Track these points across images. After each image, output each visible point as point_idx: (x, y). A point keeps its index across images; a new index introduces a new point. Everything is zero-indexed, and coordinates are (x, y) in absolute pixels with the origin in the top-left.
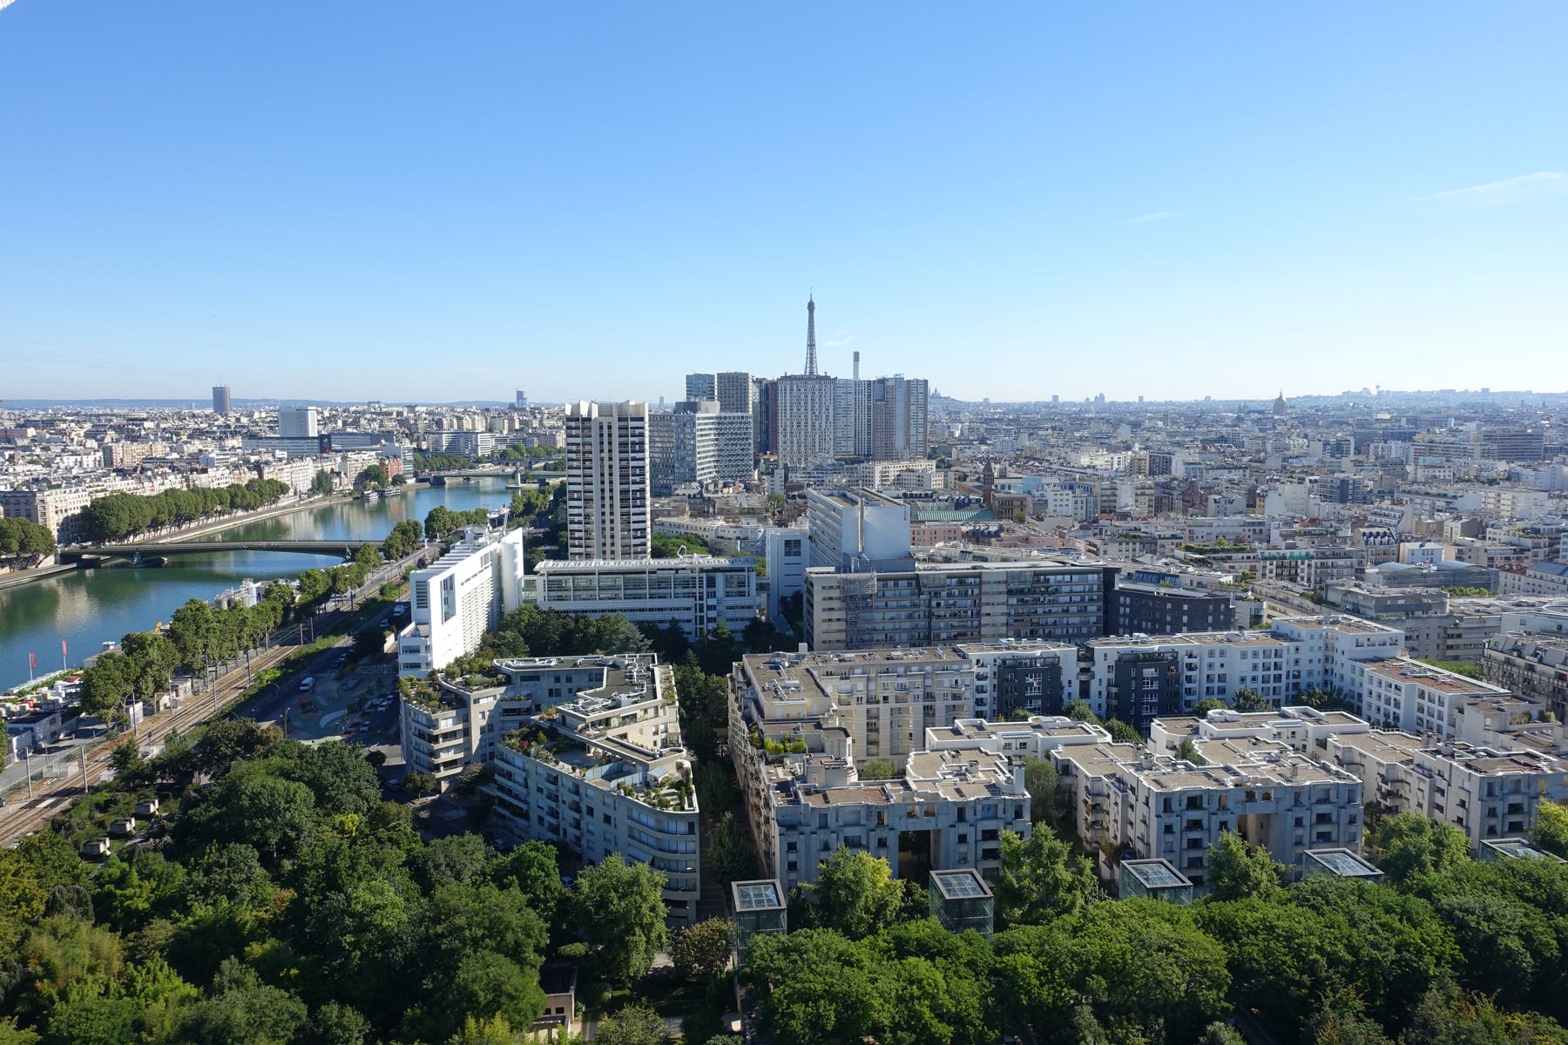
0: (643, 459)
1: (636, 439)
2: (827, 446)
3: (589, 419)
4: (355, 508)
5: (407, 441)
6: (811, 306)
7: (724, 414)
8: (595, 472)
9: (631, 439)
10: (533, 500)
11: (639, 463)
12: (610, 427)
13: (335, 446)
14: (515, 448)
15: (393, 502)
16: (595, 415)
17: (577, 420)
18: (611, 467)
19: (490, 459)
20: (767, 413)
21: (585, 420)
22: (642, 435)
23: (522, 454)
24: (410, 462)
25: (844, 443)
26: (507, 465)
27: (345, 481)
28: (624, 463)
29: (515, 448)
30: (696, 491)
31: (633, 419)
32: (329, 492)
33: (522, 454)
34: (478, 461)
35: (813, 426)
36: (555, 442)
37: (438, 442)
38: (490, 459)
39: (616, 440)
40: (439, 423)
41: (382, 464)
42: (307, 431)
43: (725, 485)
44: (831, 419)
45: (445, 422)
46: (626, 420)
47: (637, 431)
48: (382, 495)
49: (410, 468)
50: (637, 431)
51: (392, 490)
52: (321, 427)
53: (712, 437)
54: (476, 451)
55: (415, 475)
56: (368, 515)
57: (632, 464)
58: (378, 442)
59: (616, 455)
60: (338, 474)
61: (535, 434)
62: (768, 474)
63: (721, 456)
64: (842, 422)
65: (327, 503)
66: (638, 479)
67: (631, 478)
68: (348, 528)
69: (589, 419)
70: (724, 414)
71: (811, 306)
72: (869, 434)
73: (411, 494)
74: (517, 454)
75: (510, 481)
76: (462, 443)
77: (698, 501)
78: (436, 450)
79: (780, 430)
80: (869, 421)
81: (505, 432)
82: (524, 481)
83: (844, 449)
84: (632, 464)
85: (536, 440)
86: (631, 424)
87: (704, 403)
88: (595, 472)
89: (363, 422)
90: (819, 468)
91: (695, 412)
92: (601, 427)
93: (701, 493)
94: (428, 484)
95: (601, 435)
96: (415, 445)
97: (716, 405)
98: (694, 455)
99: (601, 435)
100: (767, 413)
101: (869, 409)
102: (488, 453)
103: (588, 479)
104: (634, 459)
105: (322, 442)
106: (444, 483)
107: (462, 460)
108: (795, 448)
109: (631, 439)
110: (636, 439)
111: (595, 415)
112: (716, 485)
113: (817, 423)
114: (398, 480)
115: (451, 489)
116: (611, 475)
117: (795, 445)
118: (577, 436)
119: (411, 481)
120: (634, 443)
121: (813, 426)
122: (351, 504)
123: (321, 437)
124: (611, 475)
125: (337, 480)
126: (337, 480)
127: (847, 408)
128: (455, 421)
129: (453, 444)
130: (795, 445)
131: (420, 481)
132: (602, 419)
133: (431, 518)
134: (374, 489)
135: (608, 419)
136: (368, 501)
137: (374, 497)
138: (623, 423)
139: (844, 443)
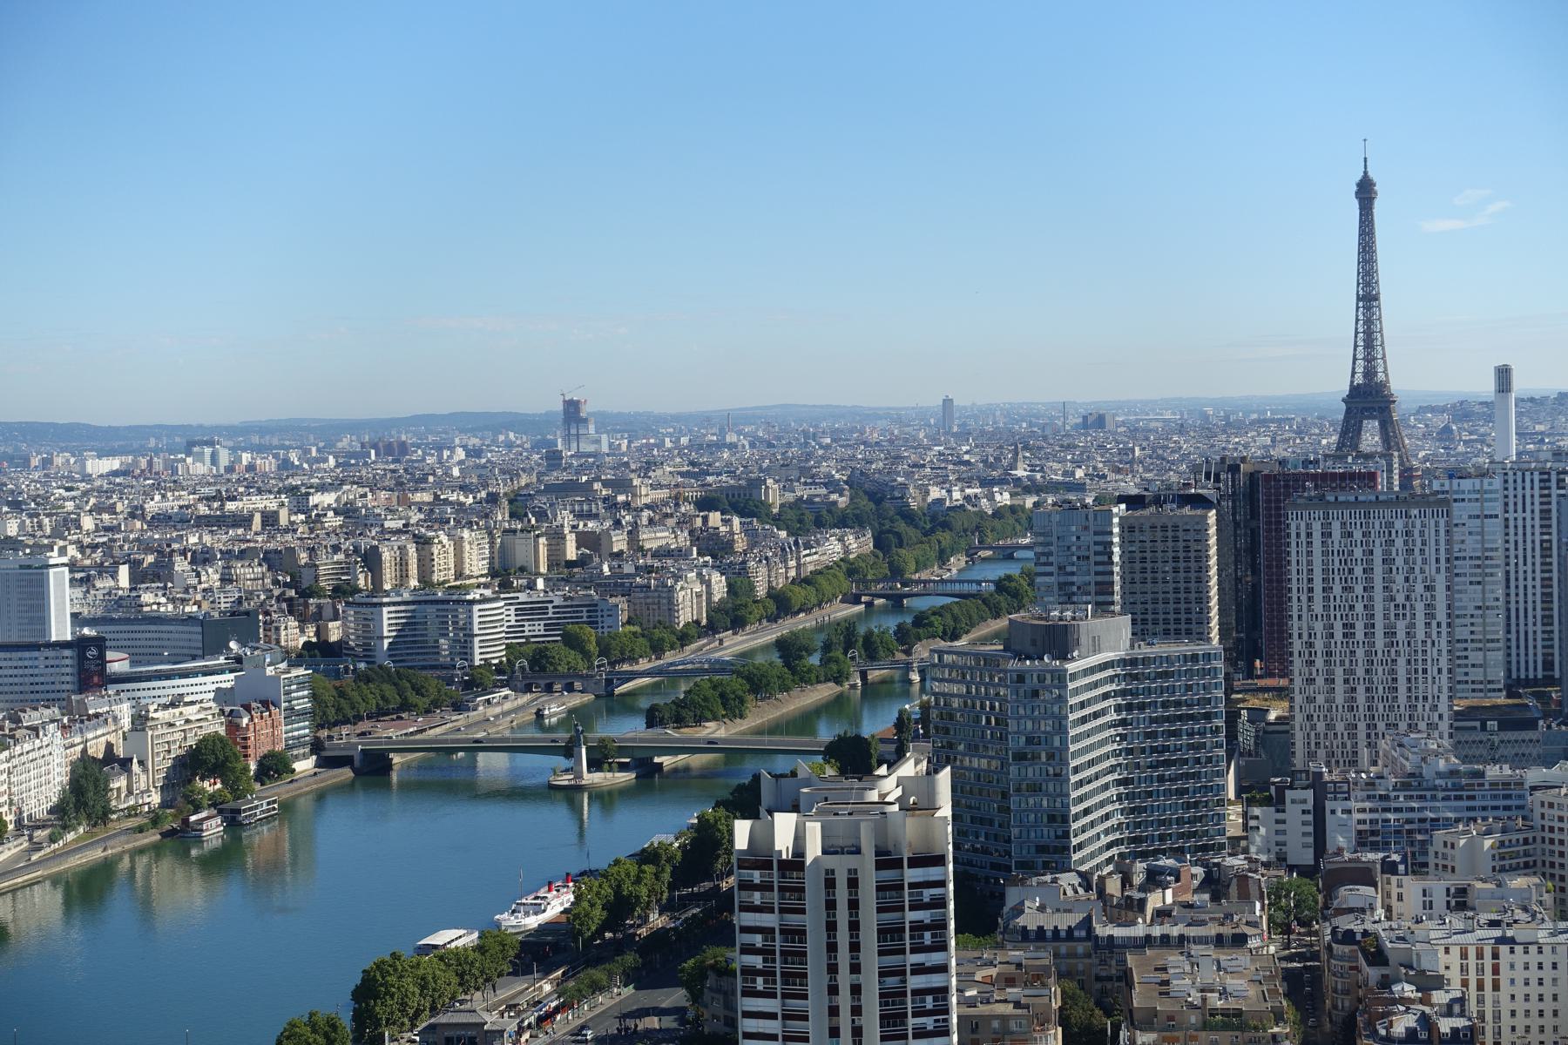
0: (943, 969)
1: (924, 916)
2: (1432, 690)
3: (796, 863)
4: (166, 864)
5: (293, 623)
6: (1365, 192)
7: (1144, 650)
8: (815, 1004)
9: (911, 916)
10: (627, 888)
11: (935, 980)
12: (853, 883)
13: (118, 663)
14: (571, 641)
15: (261, 837)
16: (813, 850)
17: (765, 865)
18: (856, 990)
19: (504, 674)
20: (1253, 549)
21: (783, 865)
22: (941, 903)
23: (586, 655)
24: (303, 713)
25: (1476, 657)
26: (549, 689)
27: (142, 781)
28: (892, 981)
29: (571, 641)
30: (1073, 919)
31: (915, 862)
32: (100, 816)
33: (586, 655)
34: (476, 683)
35: (1390, 634)
36: (671, 607)
37: (369, 633)
38: (504, 674)
39: (870, 920)
40: (371, 560)
41: (233, 727)
42: (42, 620)
43: (1155, 879)
44: (1441, 615)
45: (386, 555)
46: (897, 864)
47: (927, 894)
48: (233, 821)
49: (303, 729)
50: (927, 894)
51: (260, 802)
52: (78, 592)
53: (1112, 716)
54: (466, 653)
55: (316, 747)
56: (195, 872)
57: (915, 982)
58: (219, 647)
59: (871, 960)
60: (125, 764)
61: (619, 585)
62: (1267, 802)
63: (1136, 800)
64: (1469, 597)
65: (97, 854)
66: (929, 1022)
67: (912, 1022)
68: (146, 905)
69: (796, 863)
70: (1144, 650)
71: (1365, 192)
72: (1547, 620)
73: (304, 804)
74: (573, 656)
75: (560, 762)
76: (432, 629)
77: (1080, 948)
78: (368, 653)
79: (1297, 646)
80: (1546, 584)
81: (540, 583)
82: (595, 765)
83: (1476, 674)
84: (915, 982)
85: (622, 603)
86: (912, 875)
87: (1091, 625)
88: (815, 1004)
89: (181, 565)
90: (1412, 783)
91: (1064, 656)
92: (830, 884)
93: (1087, 923)
94: (346, 773)
95: (831, 905)
96: (310, 634)
97: (1122, 626)
98: (1060, 777)
99: (831, 905)
100: (1253, 549)
101: (1546, 551)
102: (498, 655)
103: (797, 1025)
104: (919, 970)
105: (82, 658)
106: (387, 766)
107: (431, 680)
108: (1340, 698)
109: (911, 916)
110: (924, 916)
111: (813, 850)
112: (1126, 881)
113: (1401, 626)
114: (275, 767)
115: (405, 787)
116: (856, 1011)
117: (1340, 687)
118: (765, 909)
119: (304, 766)
120: (918, 927)
121: (1390, 634)
122: (156, 849)
123: (80, 644)
124: (856, 1011)
125: (120, 783)
126: (120, 783)
127: (1482, 560)
128: (412, 550)
129: (409, 632)
130: (1340, 687)
131: (326, 762)
132: (832, 861)
133: (368, 991)
134: (215, 802)
135: (850, 861)
136: (199, 840)
137: (213, 829)
138: (889, 875)
139: (1476, 657)
